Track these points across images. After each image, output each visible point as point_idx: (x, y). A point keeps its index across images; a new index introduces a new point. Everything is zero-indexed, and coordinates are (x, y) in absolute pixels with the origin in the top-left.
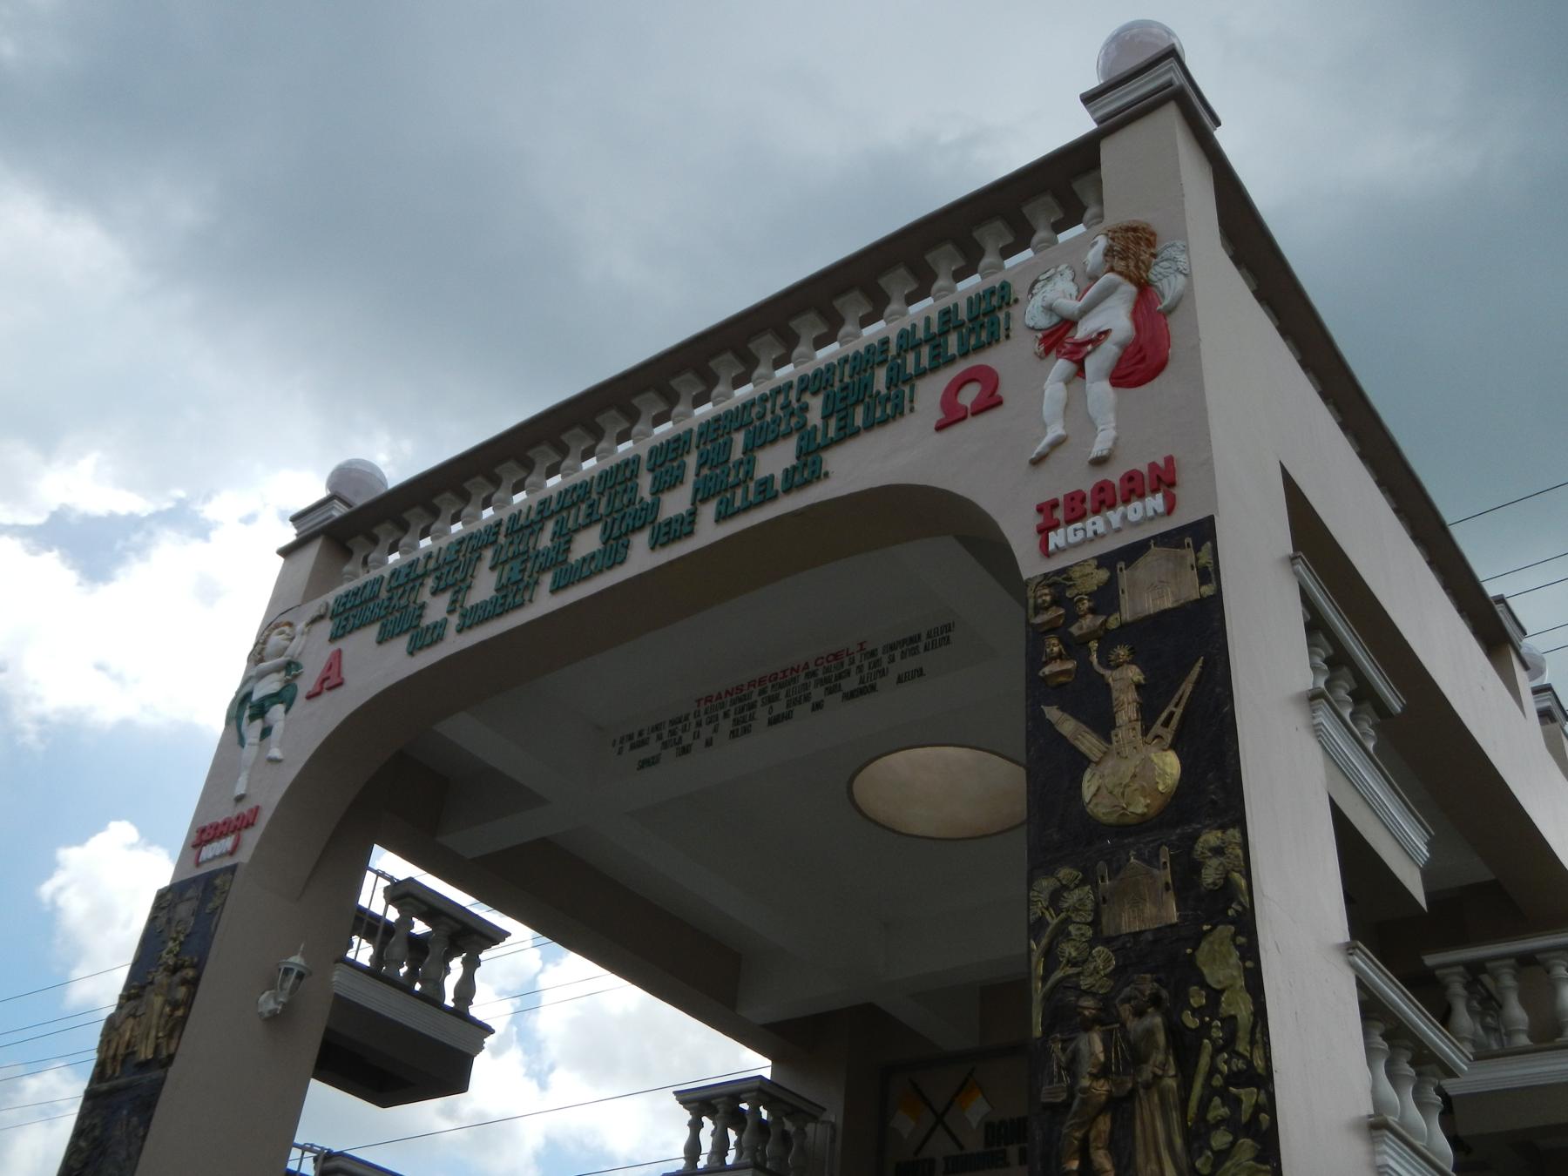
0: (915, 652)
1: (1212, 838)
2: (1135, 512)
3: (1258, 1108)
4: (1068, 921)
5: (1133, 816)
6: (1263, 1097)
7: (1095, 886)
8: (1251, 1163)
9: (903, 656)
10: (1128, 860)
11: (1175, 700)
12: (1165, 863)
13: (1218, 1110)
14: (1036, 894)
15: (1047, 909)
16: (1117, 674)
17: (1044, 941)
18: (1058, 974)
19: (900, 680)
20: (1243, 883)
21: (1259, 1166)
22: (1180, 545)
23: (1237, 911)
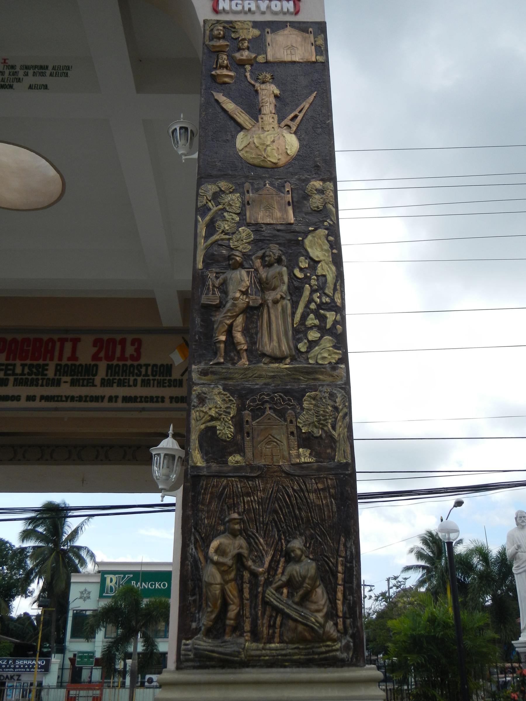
0: (43, 75)
1: (318, 184)
2: (276, 6)
3: (335, 322)
4: (224, 210)
5: (269, 163)
6: (339, 317)
7: (243, 194)
8: (331, 348)
9: (34, 74)
10: (265, 185)
11: (299, 109)
12: (288, 191)
13: (312, 320)
14: (203, 191)
15: (210, 201)
16: (263, 86)
17: (208, 218)
18: (215, 237)
19: (30, 87)
20: (334, 210)
21: (335, 351)
22: (307, 32)
23: (329, 223)
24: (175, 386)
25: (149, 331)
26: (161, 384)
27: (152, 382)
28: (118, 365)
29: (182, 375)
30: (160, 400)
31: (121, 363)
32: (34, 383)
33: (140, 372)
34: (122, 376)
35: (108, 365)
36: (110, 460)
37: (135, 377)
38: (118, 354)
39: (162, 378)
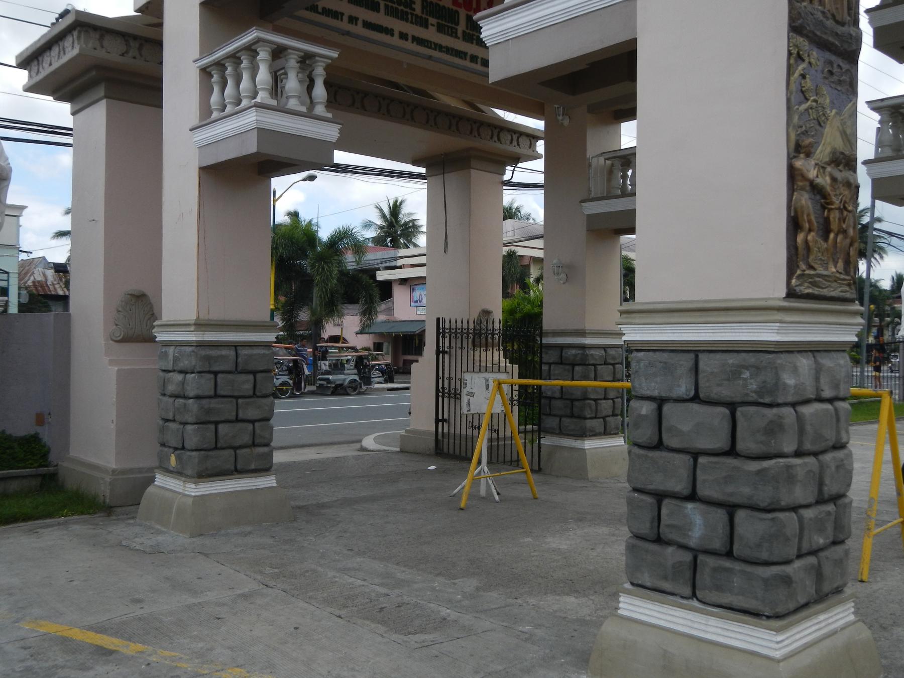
32: (403, 17)
36: (391, 116)
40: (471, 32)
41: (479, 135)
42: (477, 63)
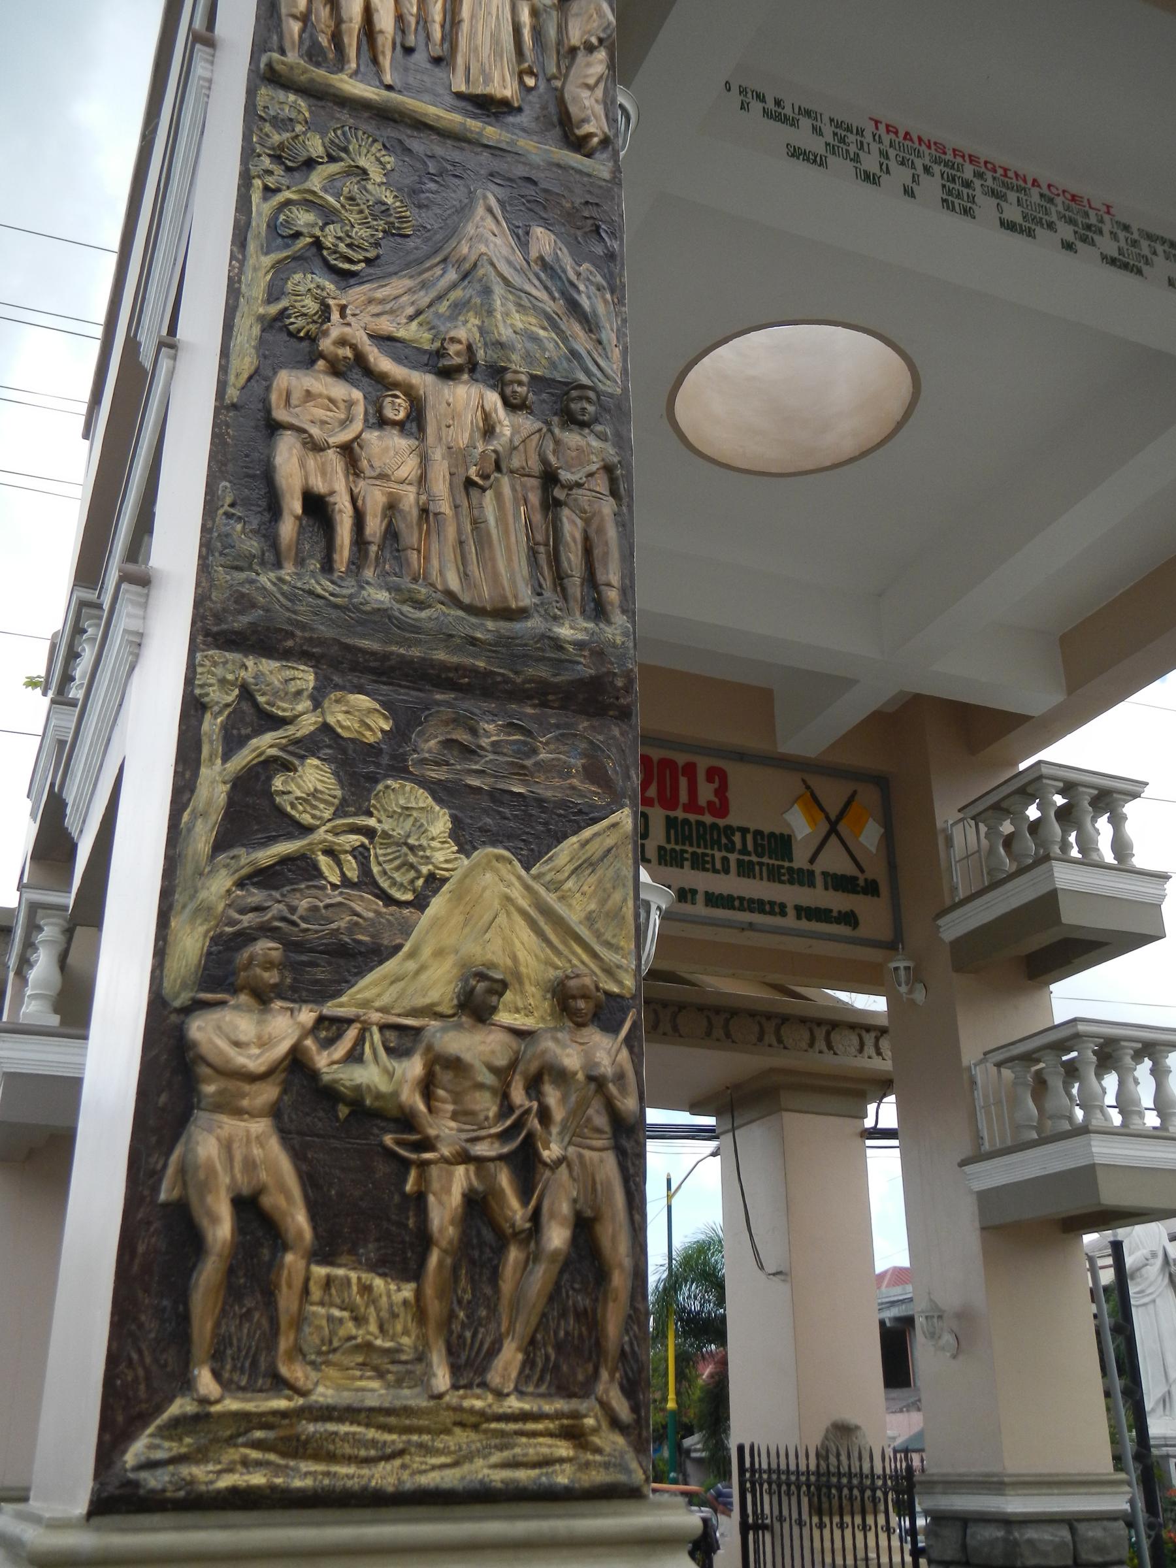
24: (801, 884)
25: (741, 756)
26: (774, 875)
27: (757, 868)
28: (686, 822)
29: (812, 861)
30: (777, 910)
31: (692, 817)
33: (733, 843)
34: (699, 847)
35: (668, 817)
37: (724, 854)
38: (684, 797)
39: (777, 863)
40: (678, 848)
41: (780, 1041)
42: (693, 903)
